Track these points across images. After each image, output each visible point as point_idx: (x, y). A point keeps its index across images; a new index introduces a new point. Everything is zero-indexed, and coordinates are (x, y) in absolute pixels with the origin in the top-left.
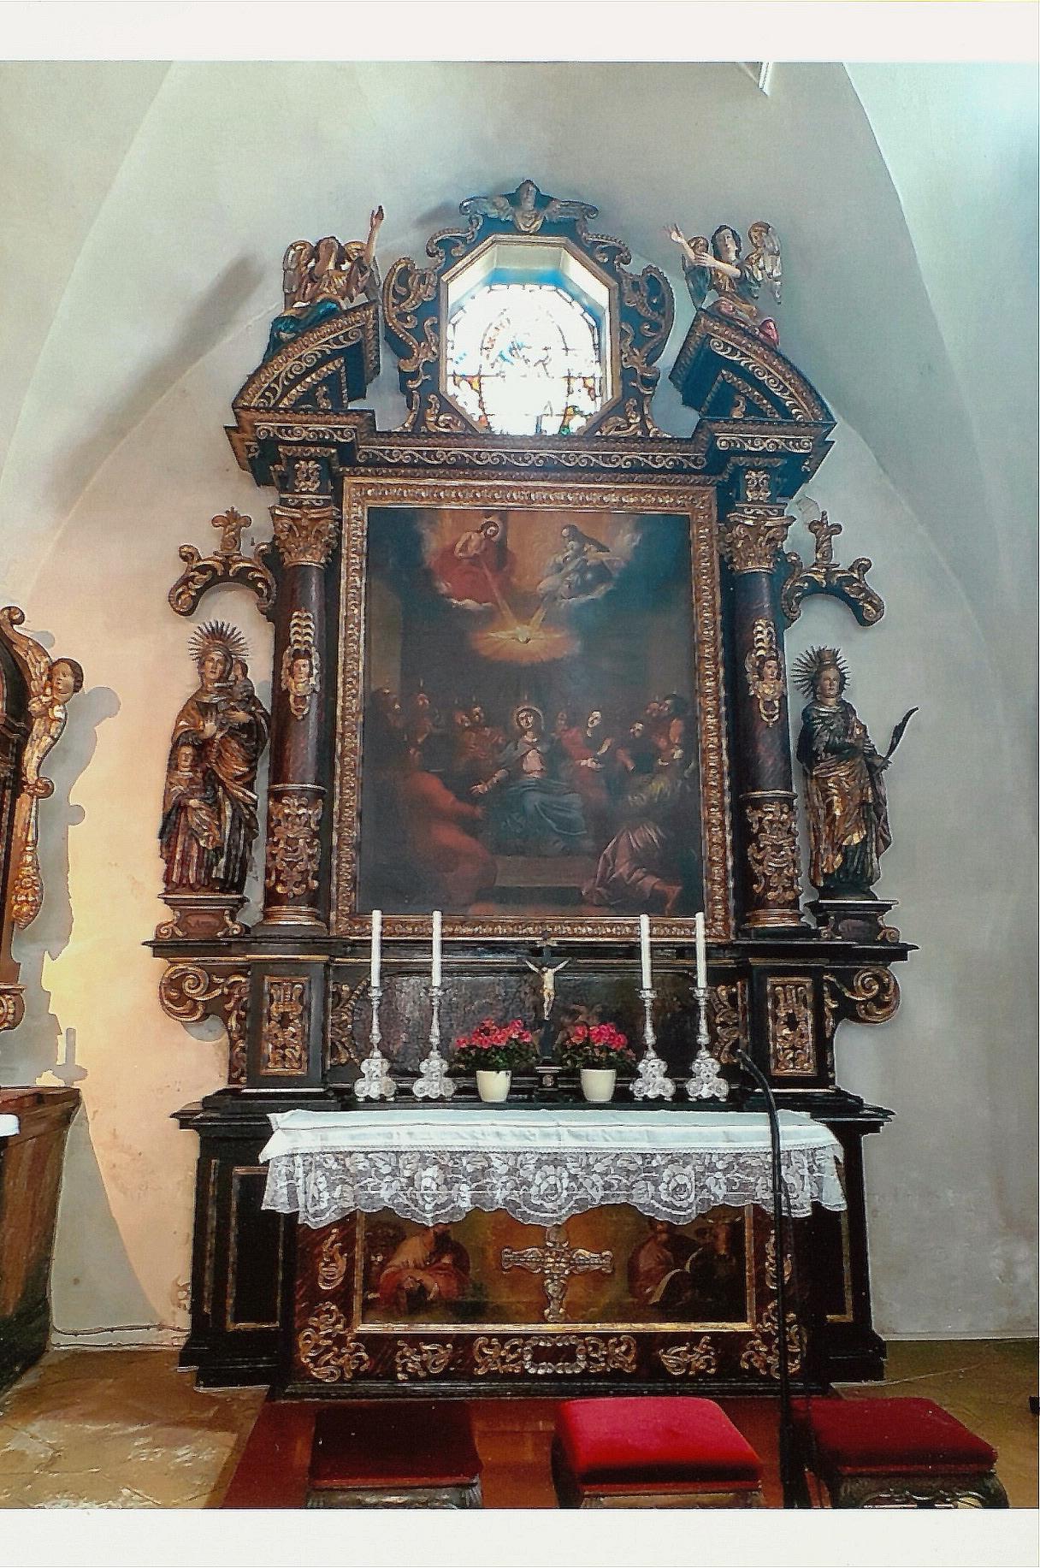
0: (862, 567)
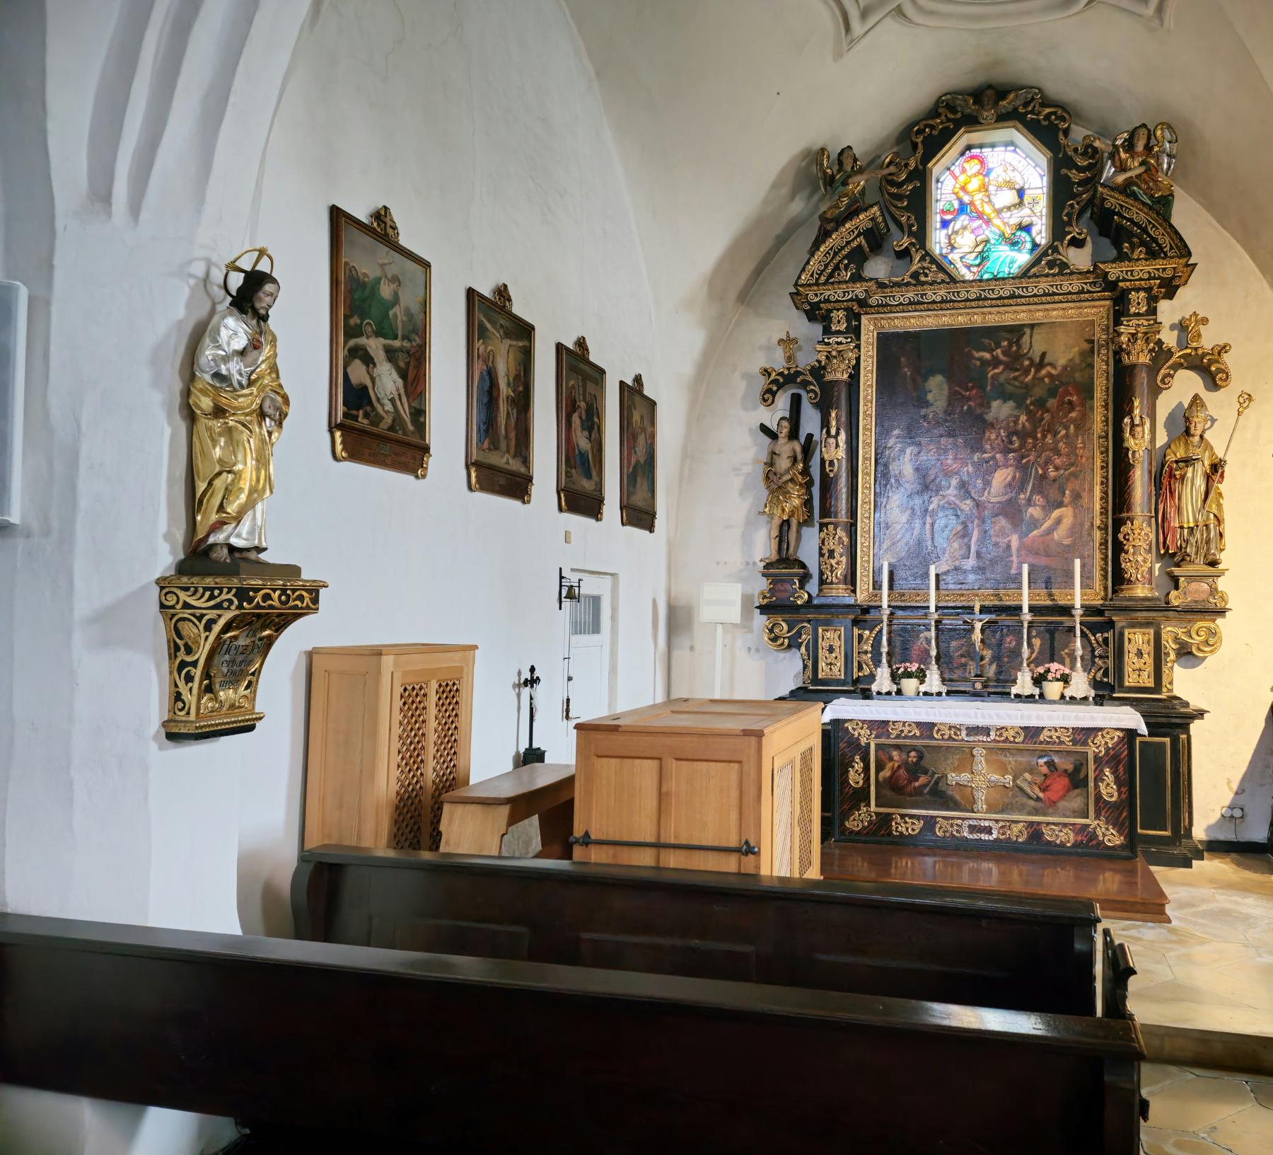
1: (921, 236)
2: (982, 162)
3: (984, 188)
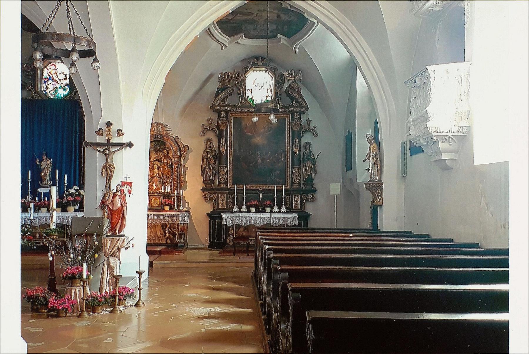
0: (315, 127)
1: (34, 86)
2: (55, 66)
3: (56, 73)
